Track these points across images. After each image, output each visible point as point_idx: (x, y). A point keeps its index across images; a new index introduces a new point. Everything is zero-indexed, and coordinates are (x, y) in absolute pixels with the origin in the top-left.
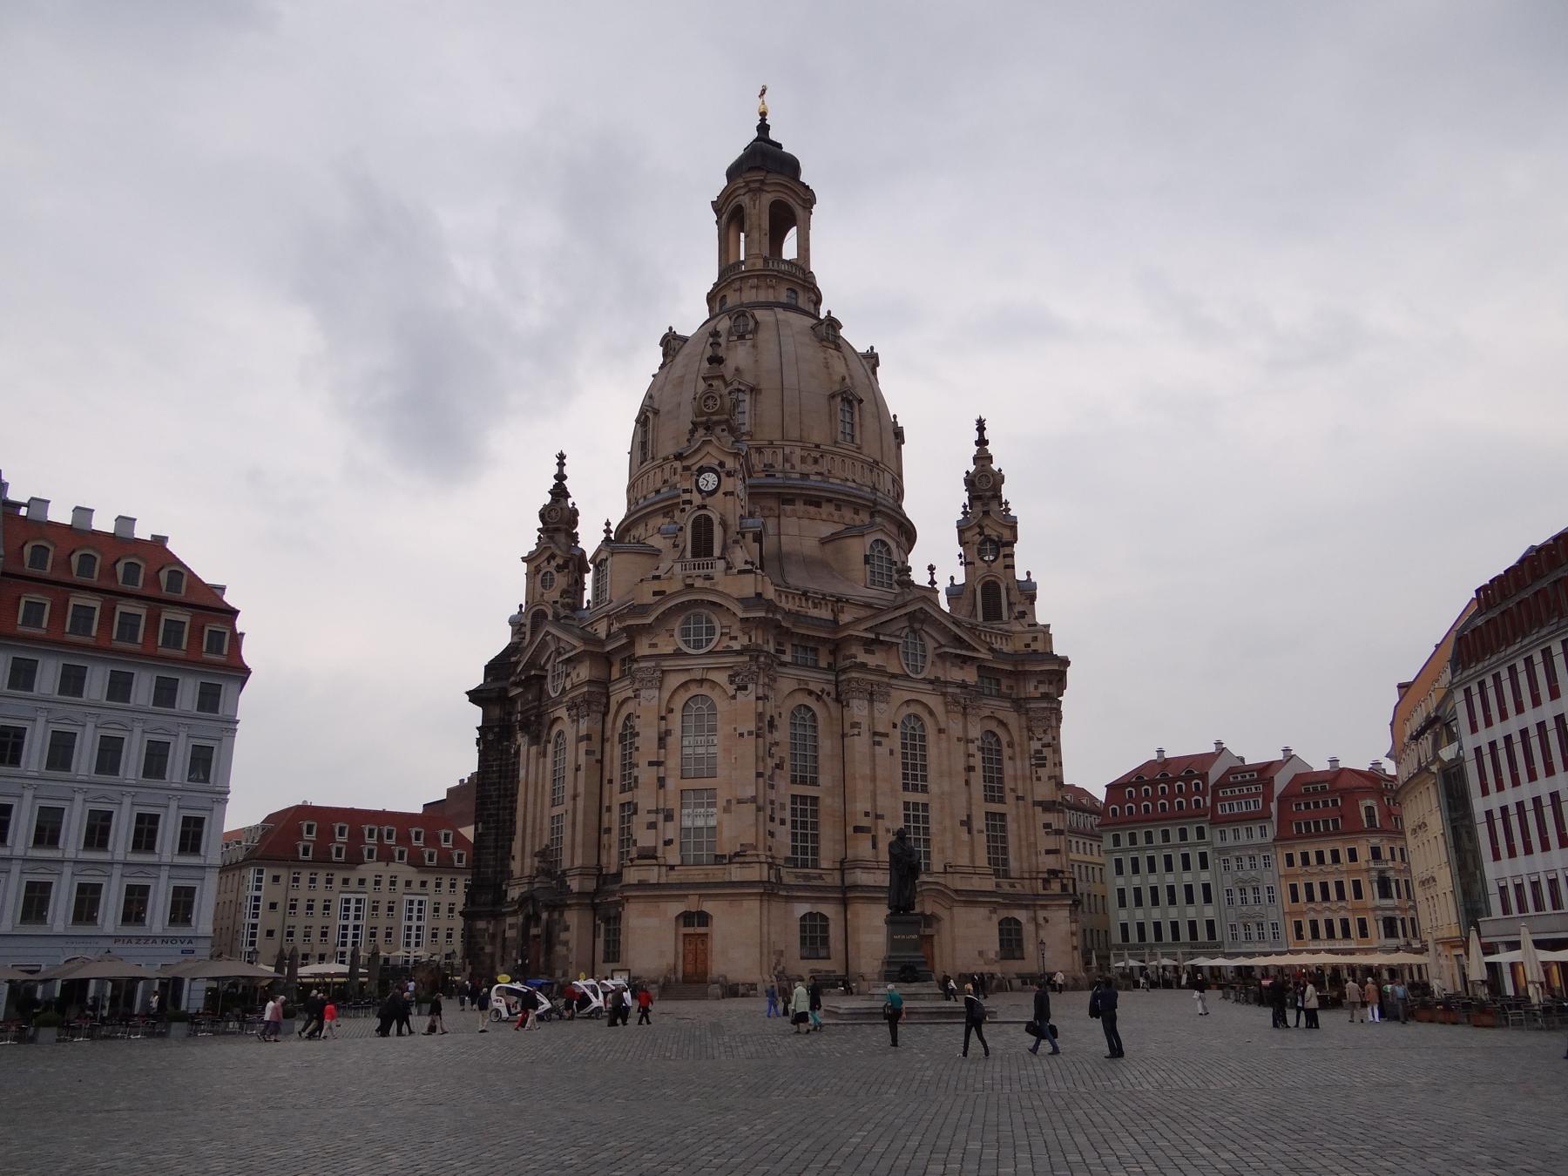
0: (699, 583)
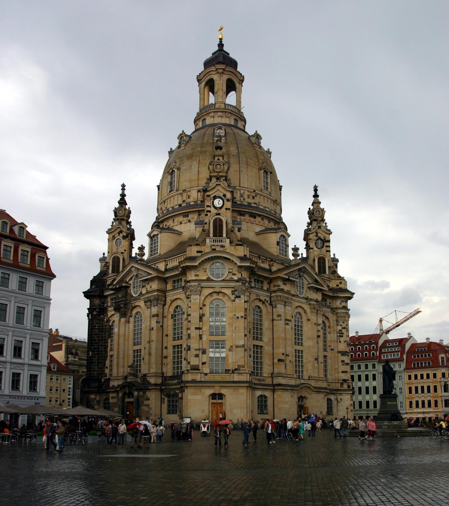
0: (218, 249)
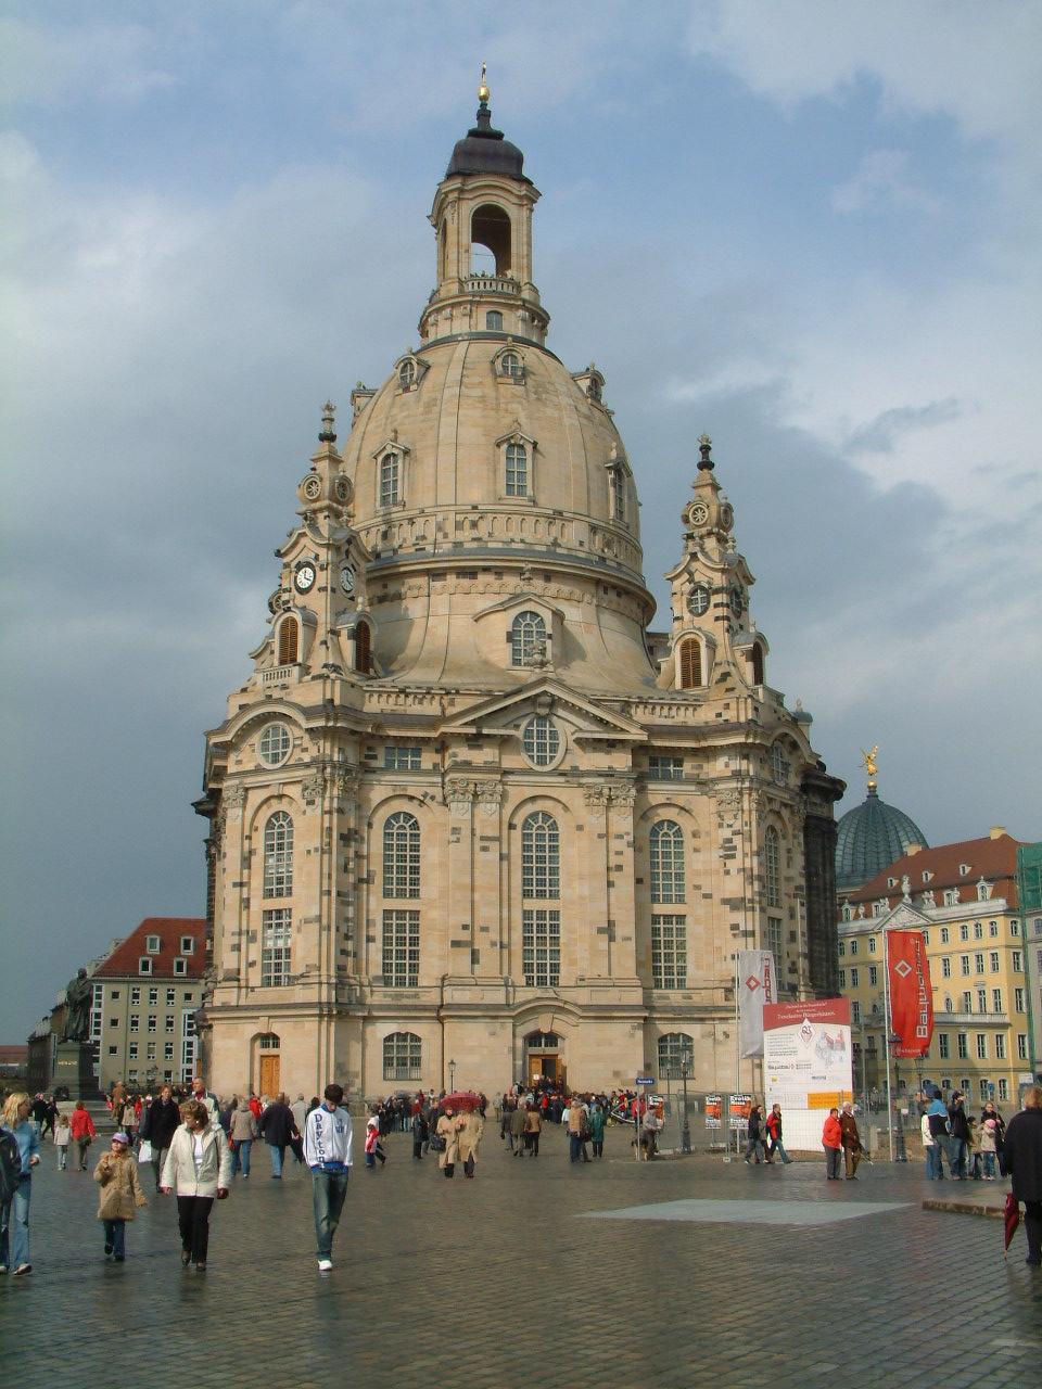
0: (276, 694)
